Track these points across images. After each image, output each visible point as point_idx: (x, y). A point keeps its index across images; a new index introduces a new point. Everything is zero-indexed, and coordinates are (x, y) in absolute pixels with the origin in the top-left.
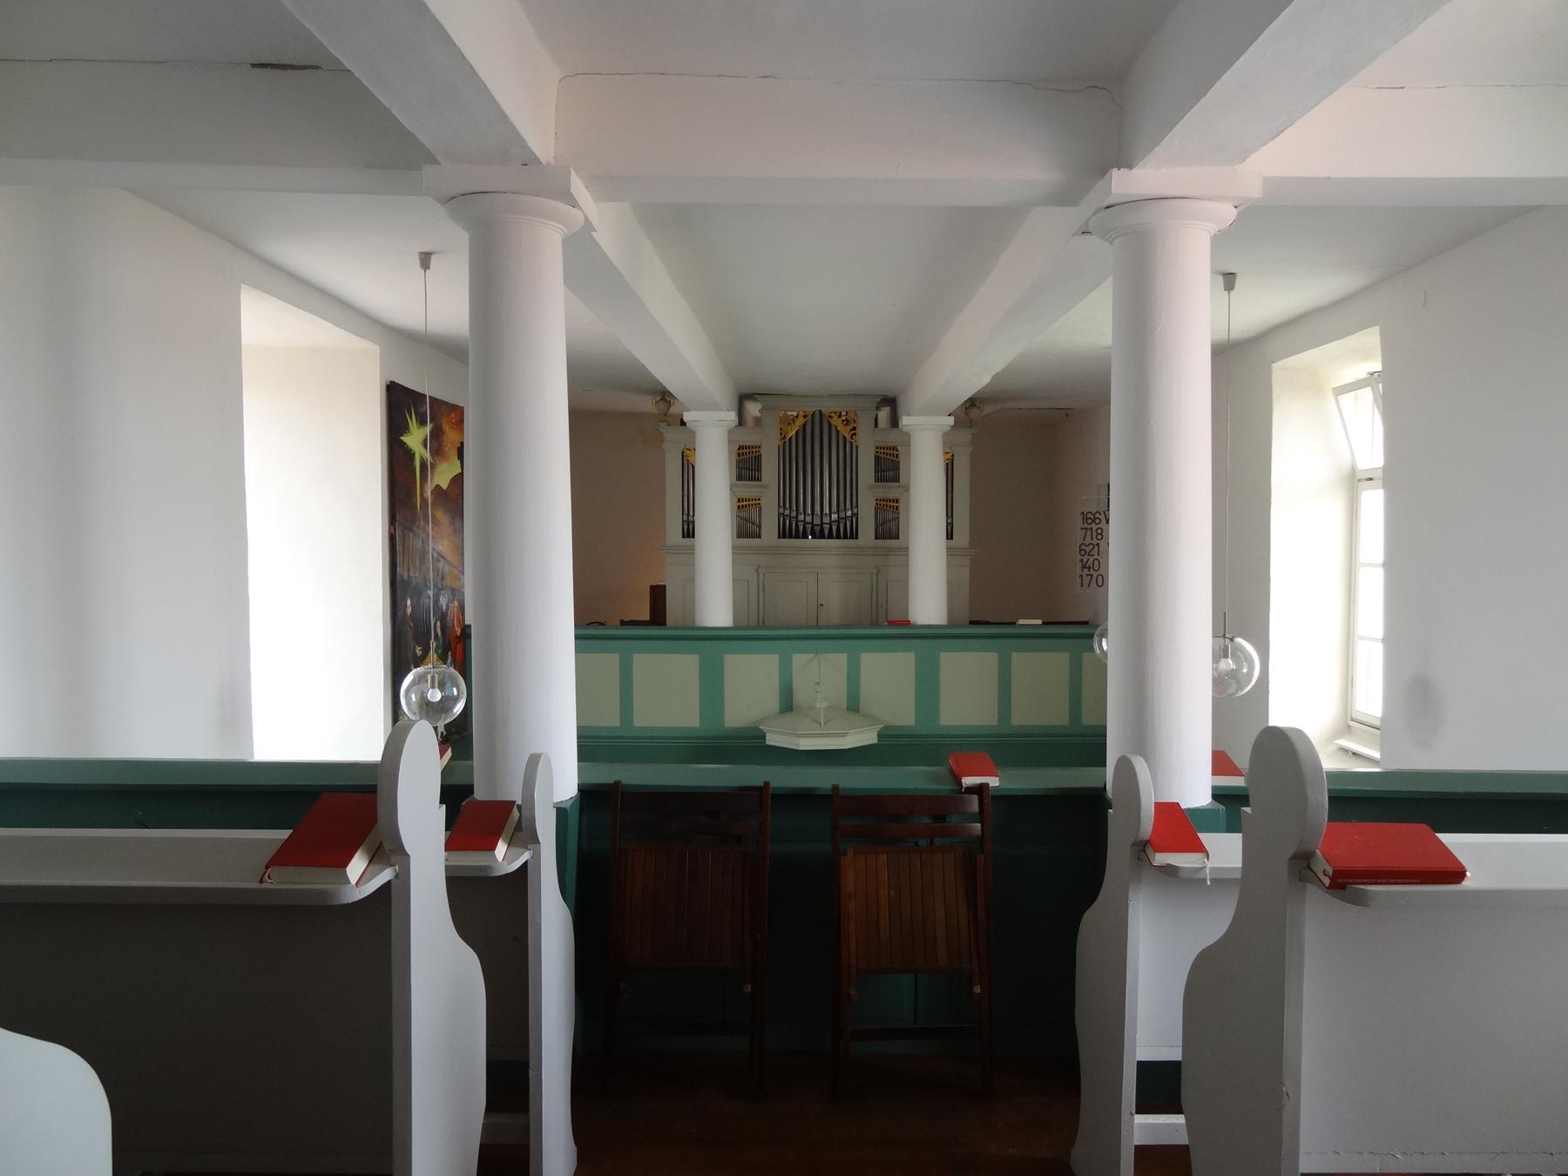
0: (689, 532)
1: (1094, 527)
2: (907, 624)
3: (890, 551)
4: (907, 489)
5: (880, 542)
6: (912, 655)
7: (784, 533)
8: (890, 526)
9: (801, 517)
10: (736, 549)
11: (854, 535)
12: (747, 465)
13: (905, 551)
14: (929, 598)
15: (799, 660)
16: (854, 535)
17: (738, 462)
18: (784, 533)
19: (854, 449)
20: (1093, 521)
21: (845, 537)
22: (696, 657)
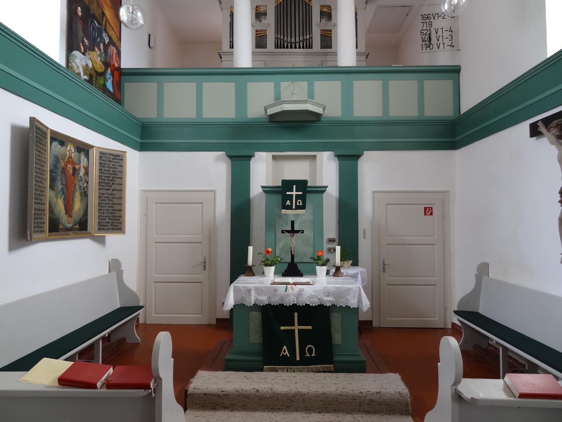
0: (232, 46)
1: (428, 21)
2: (337, 67)
3: (326, 54)
4: (335, 25)
5: (324, 50)
6: (339, 83)
7: (277, 47)
8: (327, 40)
9: (286, 38)
10: (254, 54)
11: (311, 47)
12: (259, 14)
13: (335, 54)
14: (347, 54)
15: (284, 85)
16: (311, 47)
17: (256, 13)
18: (277, 47)
19: (310, 7)
20: (427, 18)
21: (307, 48)
22: (234, 83)
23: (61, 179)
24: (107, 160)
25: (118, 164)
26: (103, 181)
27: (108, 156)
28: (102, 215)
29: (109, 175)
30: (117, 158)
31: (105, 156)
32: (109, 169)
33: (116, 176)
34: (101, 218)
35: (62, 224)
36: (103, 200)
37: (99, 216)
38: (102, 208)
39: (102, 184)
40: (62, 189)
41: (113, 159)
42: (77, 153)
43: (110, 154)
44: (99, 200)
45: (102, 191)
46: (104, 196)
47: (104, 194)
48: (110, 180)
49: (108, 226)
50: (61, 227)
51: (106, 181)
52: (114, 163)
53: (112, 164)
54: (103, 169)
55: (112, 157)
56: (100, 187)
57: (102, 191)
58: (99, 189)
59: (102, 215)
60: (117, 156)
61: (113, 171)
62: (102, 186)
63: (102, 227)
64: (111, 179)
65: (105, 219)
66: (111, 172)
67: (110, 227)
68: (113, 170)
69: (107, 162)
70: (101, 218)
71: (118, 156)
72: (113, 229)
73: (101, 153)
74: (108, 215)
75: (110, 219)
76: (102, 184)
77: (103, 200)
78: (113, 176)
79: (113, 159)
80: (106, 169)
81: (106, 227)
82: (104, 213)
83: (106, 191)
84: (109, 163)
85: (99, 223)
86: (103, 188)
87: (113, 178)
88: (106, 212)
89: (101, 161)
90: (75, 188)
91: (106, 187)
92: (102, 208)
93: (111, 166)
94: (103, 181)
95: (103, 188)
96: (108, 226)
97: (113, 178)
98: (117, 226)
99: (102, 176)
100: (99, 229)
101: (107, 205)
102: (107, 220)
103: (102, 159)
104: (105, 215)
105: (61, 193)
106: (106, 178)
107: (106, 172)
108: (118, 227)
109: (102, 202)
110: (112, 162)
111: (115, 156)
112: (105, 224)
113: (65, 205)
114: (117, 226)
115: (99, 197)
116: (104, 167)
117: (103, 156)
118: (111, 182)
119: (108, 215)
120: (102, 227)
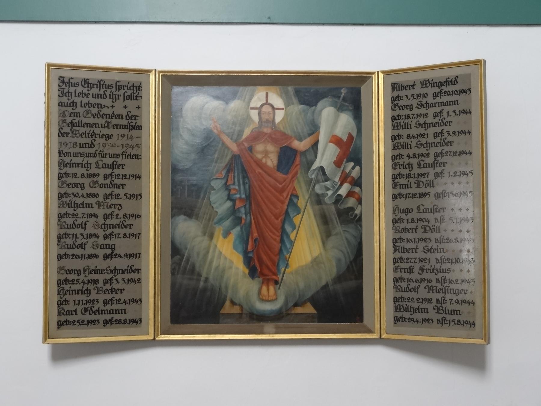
23: (226, 187)
24: (414, 103)
25: (450, 108)
26: (406, 172)
27: (418, 90)
28: (406, 276)
29: (423, 150)
30: (450, 88)
31: (409, 92)
32: (422, 131)
33: (446, 149)
34: (404, 285)
35: (233, 303)
36: (406, 230)
37: (396, 280)
38: (405, 255)
39: (403, 181)
40: (233, 211)
41: (435, 95)
42: (297, 108)
43: (425, 83)
44: (396, 230)
45: (403, 204)
46: (410, 216)
47: (408, 211)
48: (426, 166)
49: (425, 311)
50: (227, 309)
51: (416, 171)
52: (438, 109)
53: (431, 111)
54: (404, 132)
55: (430, 91)
56: (397, 191)
57: (403, 204)
58: (394, 197)
59: (406, 276)
60: (448, 82)
61: (436, 135)
62: (403, 186)
63: (407, 315)
64: (430, 160)
65: (416, 290)
66: (431, 139)
67: (432, 314)
68: (438, 129)
69: (416, 111)
70: (404, 285)
71: (454, 81)
72: (442, 322)
73: (395, 86)
74: (425, 275)
75: (430, 289)
76: (403, 181)
77: (406, 230)
78: (439, 150)
79: (435, 95)
80: (414, 131)
81: (418, 316)
82: (410, 270)
83: (417, 202)
84: (423, 111)
85: (396, 300)
86: (404, 191)
87: (436, 155)
88: (417, 267)
89: (397, 112)
90: (292, 203)
91: (414, 190)
92: (405, 255)
93: (430, 119)
94: (406, 172)
95: (404, 191)
96: (425, 311)
97: (436, 155)
98: (458, 312)
99: (400, 156)
100: (397, 320)
101: (421, 245)
102: (423, 293)
103: (401, 103)
104: (415, 276)
105: (227, 223)
106: (414, 161)
107: (414, 142)
108: (462, 318)
109: (405, 236)
110: (432, 105)
111: (440, 84)
112: (415, 305)
113: (245, 253)
114: (458, 312)
115: (395, 222)
116: (407, 126)
117: (402, 93)
118: (431, 171)
119: (425, 275)
120: (407, 315)
